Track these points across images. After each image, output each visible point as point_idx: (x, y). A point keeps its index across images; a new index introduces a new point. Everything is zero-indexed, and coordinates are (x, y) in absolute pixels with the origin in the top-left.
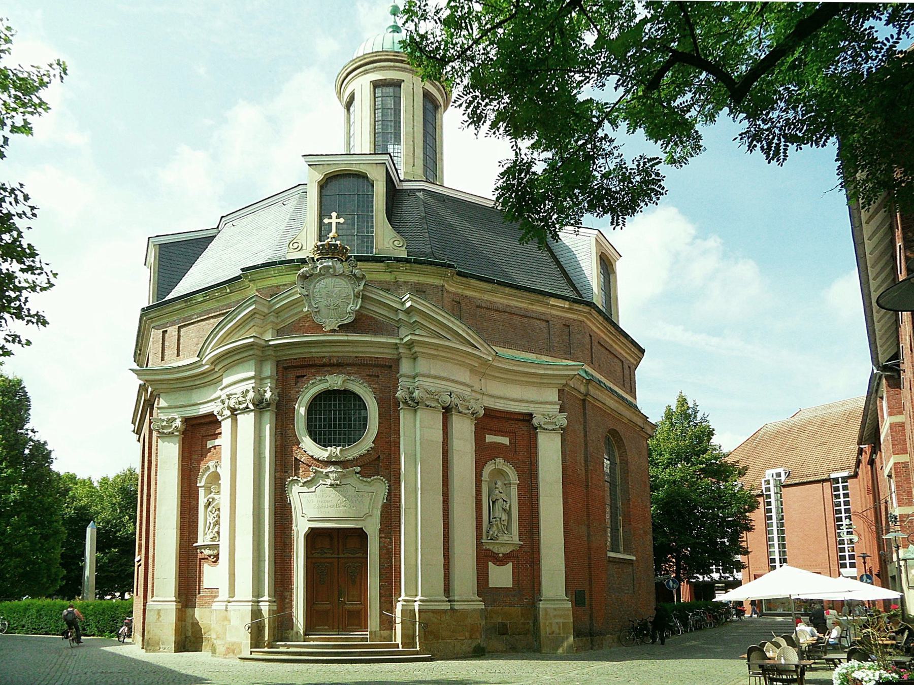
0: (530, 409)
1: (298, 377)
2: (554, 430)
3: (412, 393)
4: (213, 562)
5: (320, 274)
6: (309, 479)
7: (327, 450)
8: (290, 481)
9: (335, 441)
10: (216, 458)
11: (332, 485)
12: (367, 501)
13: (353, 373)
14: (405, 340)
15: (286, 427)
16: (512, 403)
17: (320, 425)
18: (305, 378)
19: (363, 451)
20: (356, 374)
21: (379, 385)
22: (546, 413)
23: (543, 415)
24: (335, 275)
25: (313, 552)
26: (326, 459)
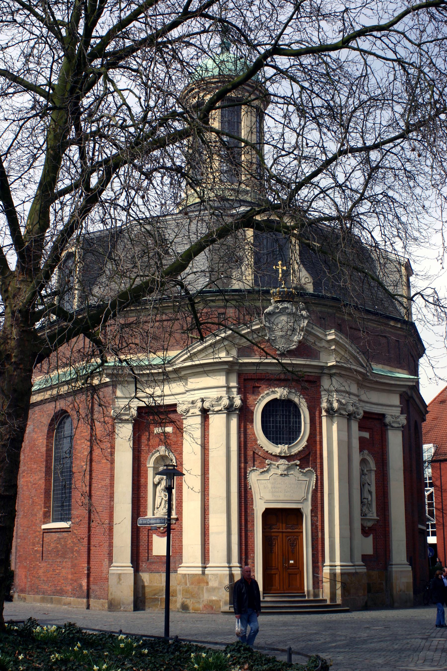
0: (383, 410)
2: (398, 427)
4: (162, 533)
5: (278, 313)
6: (265, 469)
7: (278, 447)
8: (251, 471)
9: (283, 440)
11: (281, 475)
16: (375, 406)
21: (308, 396)
22: (393, 414)
23: (392, 415)
24: (289, 314)
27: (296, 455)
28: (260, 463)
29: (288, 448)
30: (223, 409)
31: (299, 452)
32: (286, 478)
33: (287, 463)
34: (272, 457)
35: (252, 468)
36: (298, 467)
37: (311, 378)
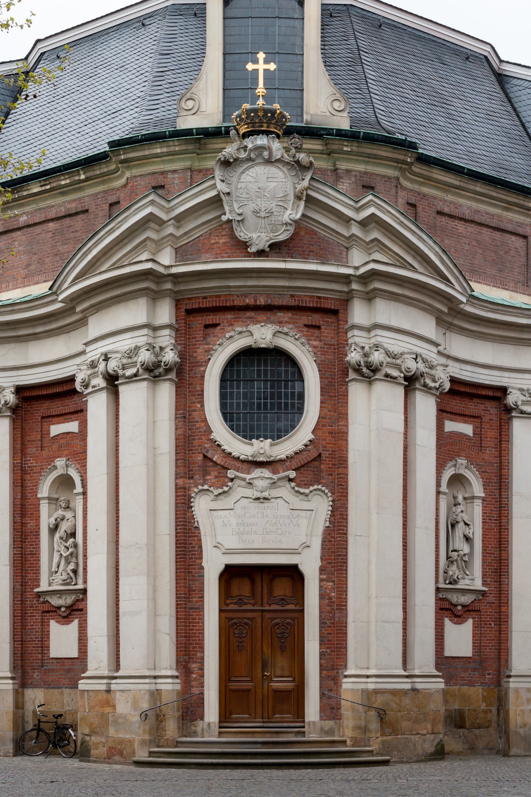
1: (207, 326)
3: (366, 355)
7: (252, 445)
10: (66, 452)
12: (304, 522)
13: (286, 322)
14: (362, 271)
15: (189, 407)
17: (238, 404)
18: (218, 328)
19: (300, 446)
20: (289, 323)
25: (228, 602)
26: (250, 458)
27: (289, 458)
28: (216, 477)
29: (272, 445)
30: (141, 371)
31: (296, 453)
32: (266, 504)
33: (271, 475)
34: (239, 465)
35: (200, 487)
36: (293, 484)
37: (326, 305)
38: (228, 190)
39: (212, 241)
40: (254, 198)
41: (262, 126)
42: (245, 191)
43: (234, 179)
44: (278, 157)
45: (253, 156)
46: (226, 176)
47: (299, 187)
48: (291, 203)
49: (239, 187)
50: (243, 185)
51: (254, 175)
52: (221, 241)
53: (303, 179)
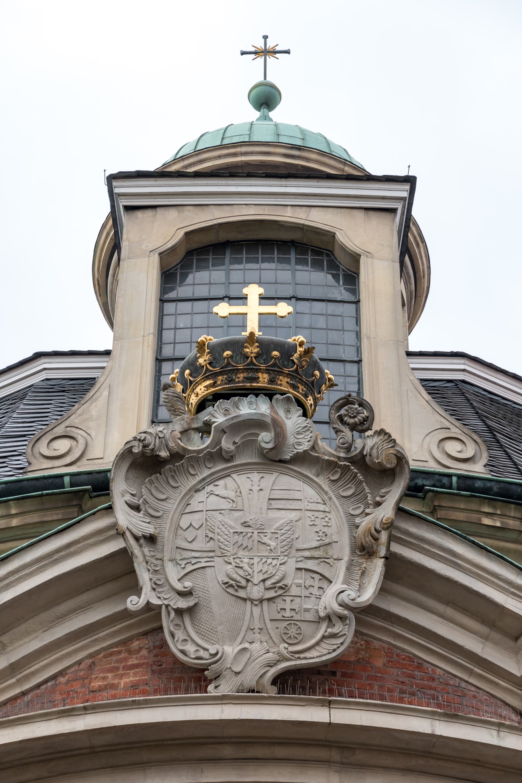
38: (150, 530)
39: (96, 684)
40: (231, 549)
41: (256, 379)
42: (201, 533)
43: (172, 506)
44: (301, 449)
45: (226, 444)
46: (146, 495)
47: (365, 523)
48: (342, 566)
49: (184, 524)
50: (196, 519)
51: (231, 494)
52: (123, 682)
53: (378, 504)
